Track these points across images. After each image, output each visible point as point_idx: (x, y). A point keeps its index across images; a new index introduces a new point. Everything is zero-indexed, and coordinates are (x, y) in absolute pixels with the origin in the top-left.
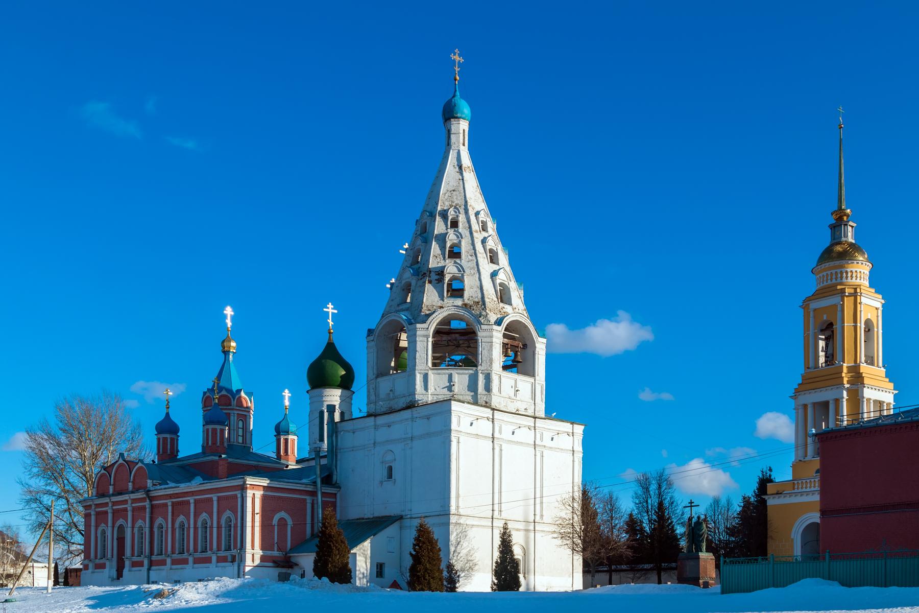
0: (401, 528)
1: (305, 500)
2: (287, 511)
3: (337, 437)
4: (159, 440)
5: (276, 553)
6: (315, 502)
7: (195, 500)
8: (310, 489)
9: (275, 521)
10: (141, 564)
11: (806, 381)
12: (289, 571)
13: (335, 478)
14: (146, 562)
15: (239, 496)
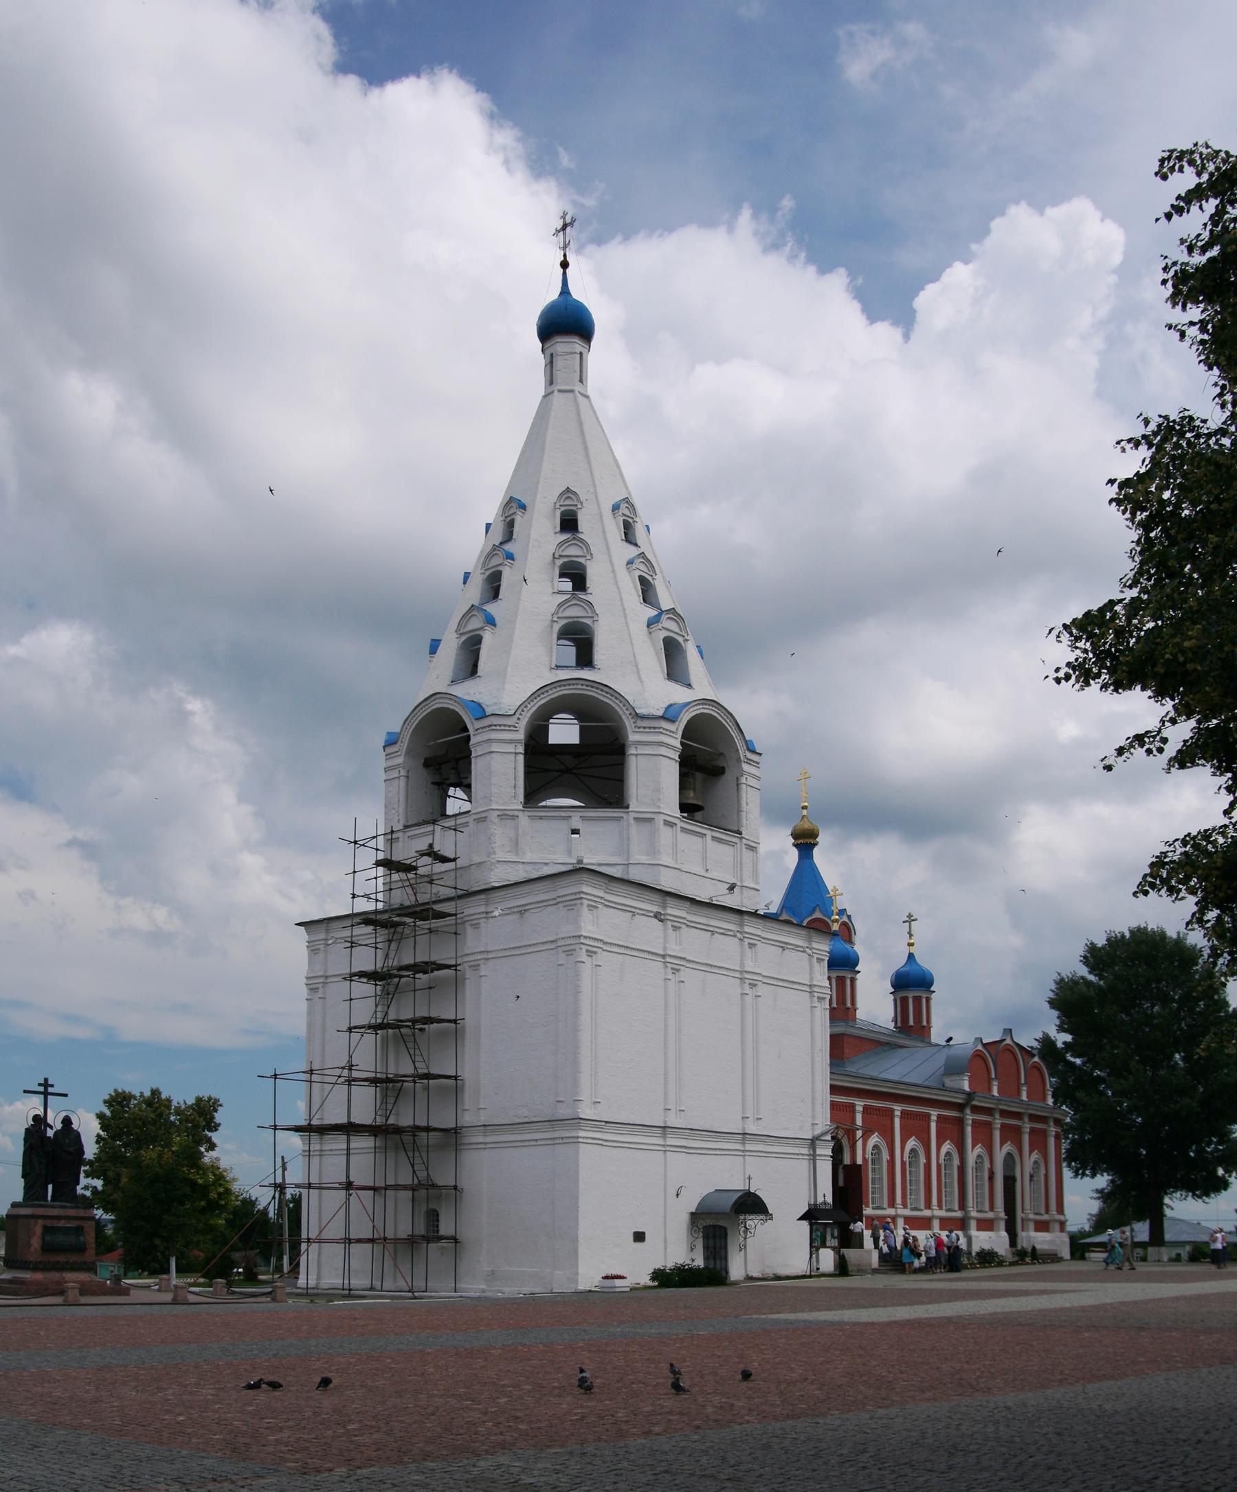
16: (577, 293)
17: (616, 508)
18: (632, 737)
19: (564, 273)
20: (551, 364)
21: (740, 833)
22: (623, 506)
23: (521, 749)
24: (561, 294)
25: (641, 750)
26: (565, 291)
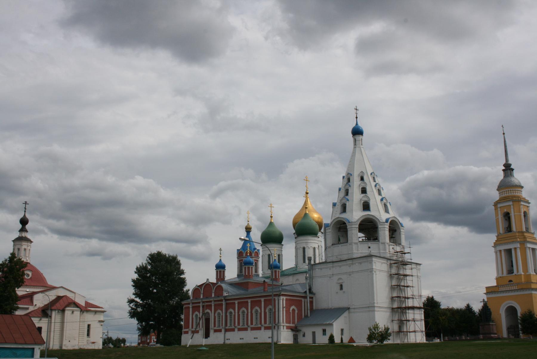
0: (349, 312)
2: (295, 306)
3: (312, 271)
4: (217, 272)
5: (291, 325)
6: (306, 301)
7: (251, 301)
8: (303, 295)
9: (291, 311)
10: (220, 331)
11: (499, 240)
12: (297, 333)
13: (312, 289)
14: (223, 330)
16: (359, 124)
17: (371, 174)
18: (380, 226)
19: (357, 120)
20: (355, 140)
21: (401, 244)
22: (373, 174)
23: (358, 229)
24: (356, 125)
25: (381, 229)
26: (357, 124)
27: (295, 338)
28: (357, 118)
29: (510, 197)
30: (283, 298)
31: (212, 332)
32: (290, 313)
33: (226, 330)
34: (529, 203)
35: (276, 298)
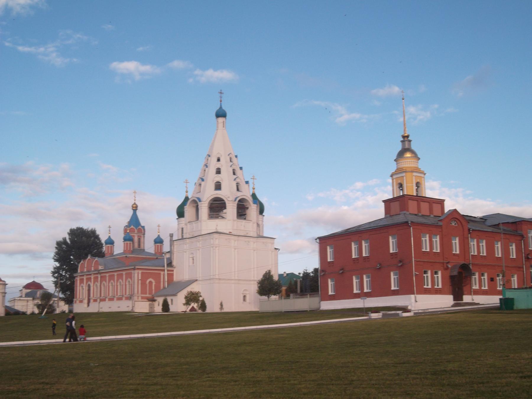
1: (160, 273)
5: (148, 295)
14: (98, 300)
15: (133, 273)
16: (224, 108)
27: (151, 307)
28: (221, 101)
29: (404, 169)
30: (138, 272)
31: (92, 301)
32: (147, 285)
33: (102, 300)
34: (425, 174)
35: (133, 271)
